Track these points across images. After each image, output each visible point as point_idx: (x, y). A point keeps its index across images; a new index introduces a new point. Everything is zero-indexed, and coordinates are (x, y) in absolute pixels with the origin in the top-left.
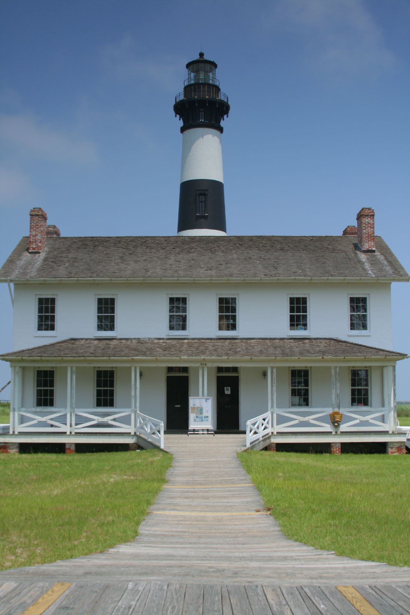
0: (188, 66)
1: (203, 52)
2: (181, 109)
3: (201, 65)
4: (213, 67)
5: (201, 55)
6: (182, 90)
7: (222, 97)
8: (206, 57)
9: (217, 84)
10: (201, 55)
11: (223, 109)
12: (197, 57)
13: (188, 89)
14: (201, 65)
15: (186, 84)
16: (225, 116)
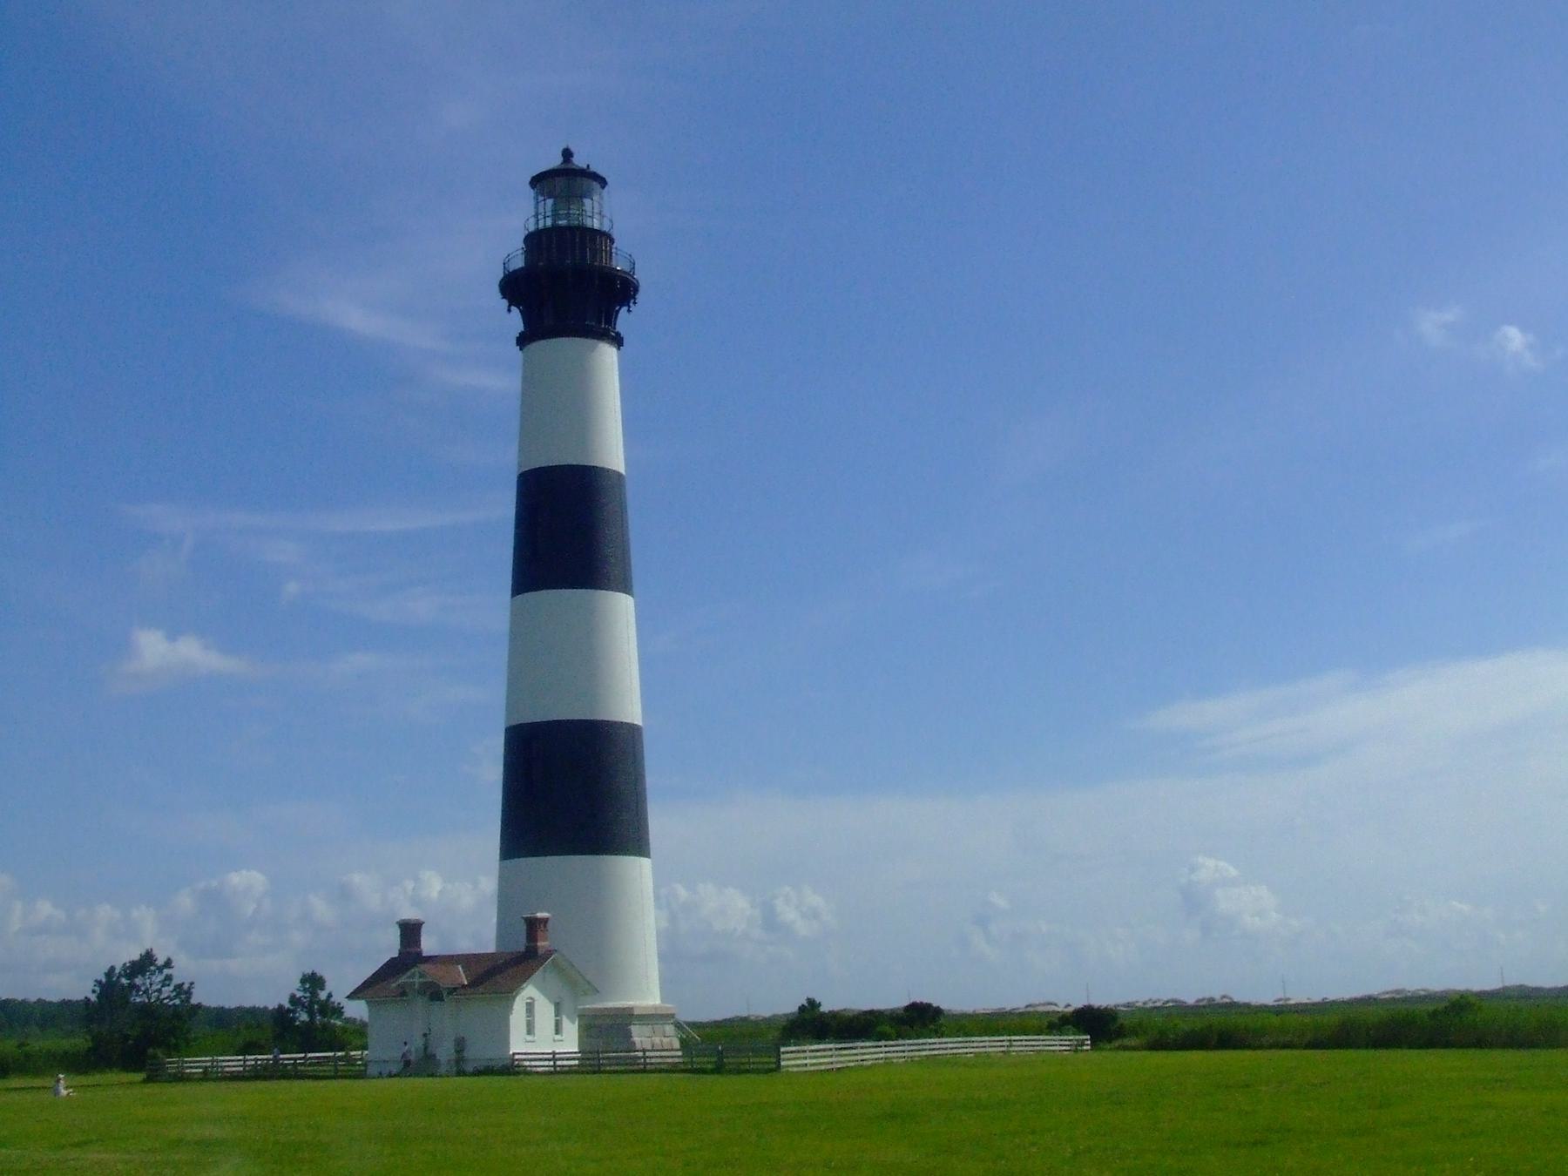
0: (538, 181)
1: (573, 149)
2: (514, 287)
3: (565, 181)
4: (596, 185)
5: (567, 154)
6: (520, 244)
7: (620, 265)
8: (579, 161)
9: (606, 228)
10: (567, 154)
11: (622, 290)
12: (556, 161)
13: (534, 241)
14: (565, 181)
15: (532, 228)
16: (625, 309)
